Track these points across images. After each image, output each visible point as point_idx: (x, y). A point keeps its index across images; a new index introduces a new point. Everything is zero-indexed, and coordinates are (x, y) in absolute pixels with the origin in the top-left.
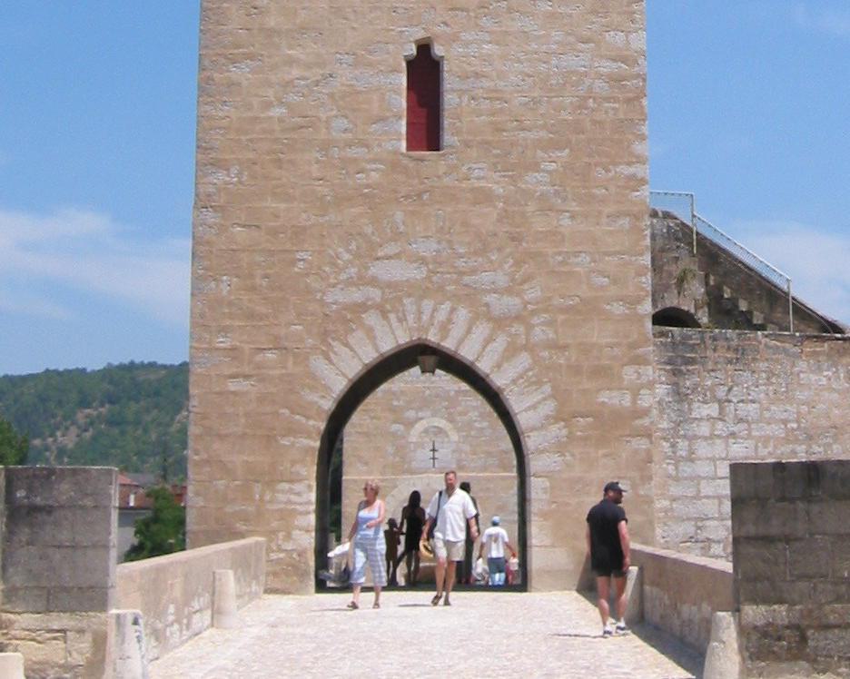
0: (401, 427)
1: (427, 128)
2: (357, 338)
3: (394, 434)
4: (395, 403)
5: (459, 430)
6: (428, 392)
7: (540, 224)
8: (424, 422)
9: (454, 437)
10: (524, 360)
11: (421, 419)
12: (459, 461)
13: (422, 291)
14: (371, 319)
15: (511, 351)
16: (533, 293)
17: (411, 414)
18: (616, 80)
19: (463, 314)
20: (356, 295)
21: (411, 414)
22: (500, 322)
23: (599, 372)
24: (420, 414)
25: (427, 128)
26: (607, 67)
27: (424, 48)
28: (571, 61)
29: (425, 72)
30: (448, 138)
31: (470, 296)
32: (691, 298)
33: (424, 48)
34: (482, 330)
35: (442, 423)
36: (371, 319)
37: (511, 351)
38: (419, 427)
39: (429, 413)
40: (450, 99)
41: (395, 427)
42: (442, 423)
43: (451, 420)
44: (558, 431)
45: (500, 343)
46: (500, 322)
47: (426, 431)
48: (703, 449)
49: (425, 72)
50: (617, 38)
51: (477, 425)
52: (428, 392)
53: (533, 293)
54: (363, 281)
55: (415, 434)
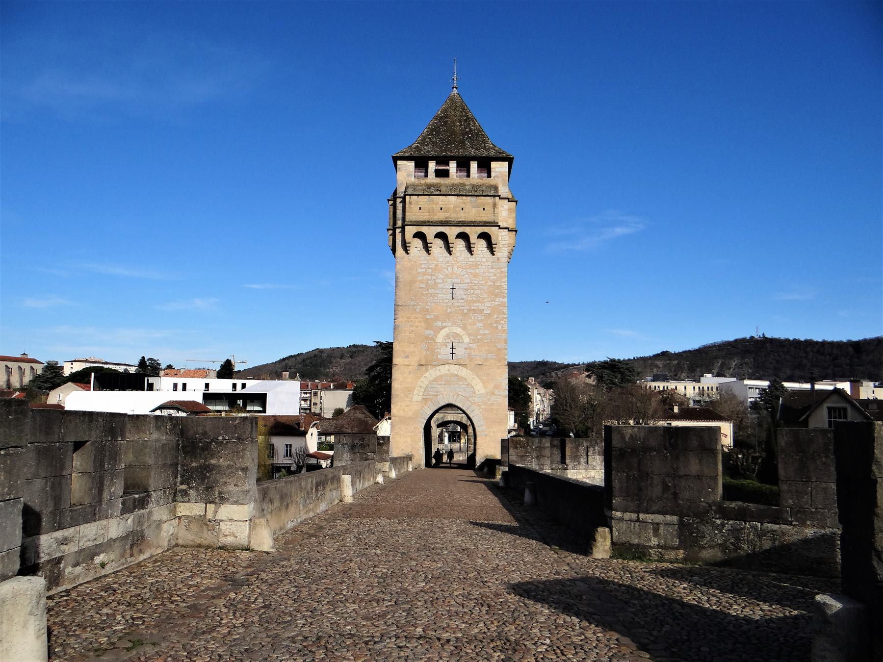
0: (432, 332)
3: (427, 337)
4: (428, 316)
5: (469, 335)
6: (449, 310)
8: (446, 329)
9: (466, 340)
11: (445, 327)
12: (469, 355)
17: (439, 323)
21: (439, 323)
24: (444, 324)
35: (459, 330)
38: (443, 333)
39: (450, 324)
41: (427, 332)
42: (459, 330)
43: (464, 328)
47: (448, 336)
51: (482, 332)
52: (449, 310)
55: (440, 339)
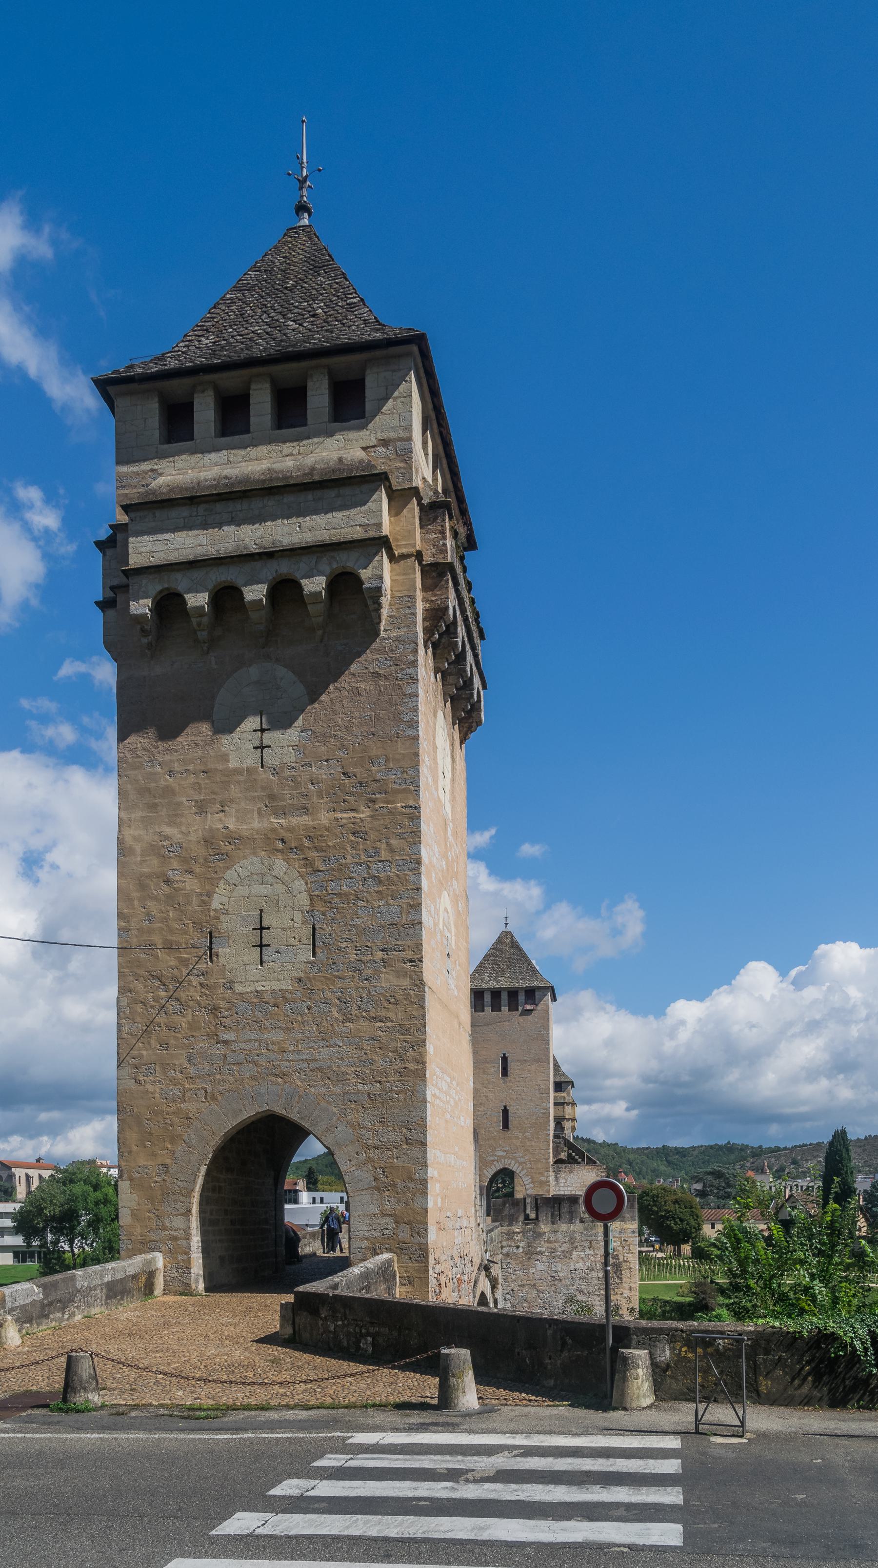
1: (506, 1125)
2: (493, 1167)
7: (528, 1143)
10: (525, 1171)
13: (504, 1157)
14: (495, 1163)
15: (523, 1169)
16: (527, 1158)
18: (544, 1113)
19: (513, 1162)
20: (492, 1158)
22: (520, 1164)
23: (540, 1173)
25: (506, 1125)
26: (542, 1111)
27: (505, 1107)
28: (534, 1110)
29: (505, 1112)
30: (510, 1126)
31: (514, 1158)
32: (563, 1156)
33: (505, 1107)
34: (517, 1165)
36: (495, 1163)
37: (523, 1169)
40: (510, 1118)
44: (531, 1185)
45: (520, 1168)
46: (520, 1164)
48: (562, 1189)
49: (505, 1112)
50: (544, 1105)
53: (527, 1158)
54: (494, 1155)
